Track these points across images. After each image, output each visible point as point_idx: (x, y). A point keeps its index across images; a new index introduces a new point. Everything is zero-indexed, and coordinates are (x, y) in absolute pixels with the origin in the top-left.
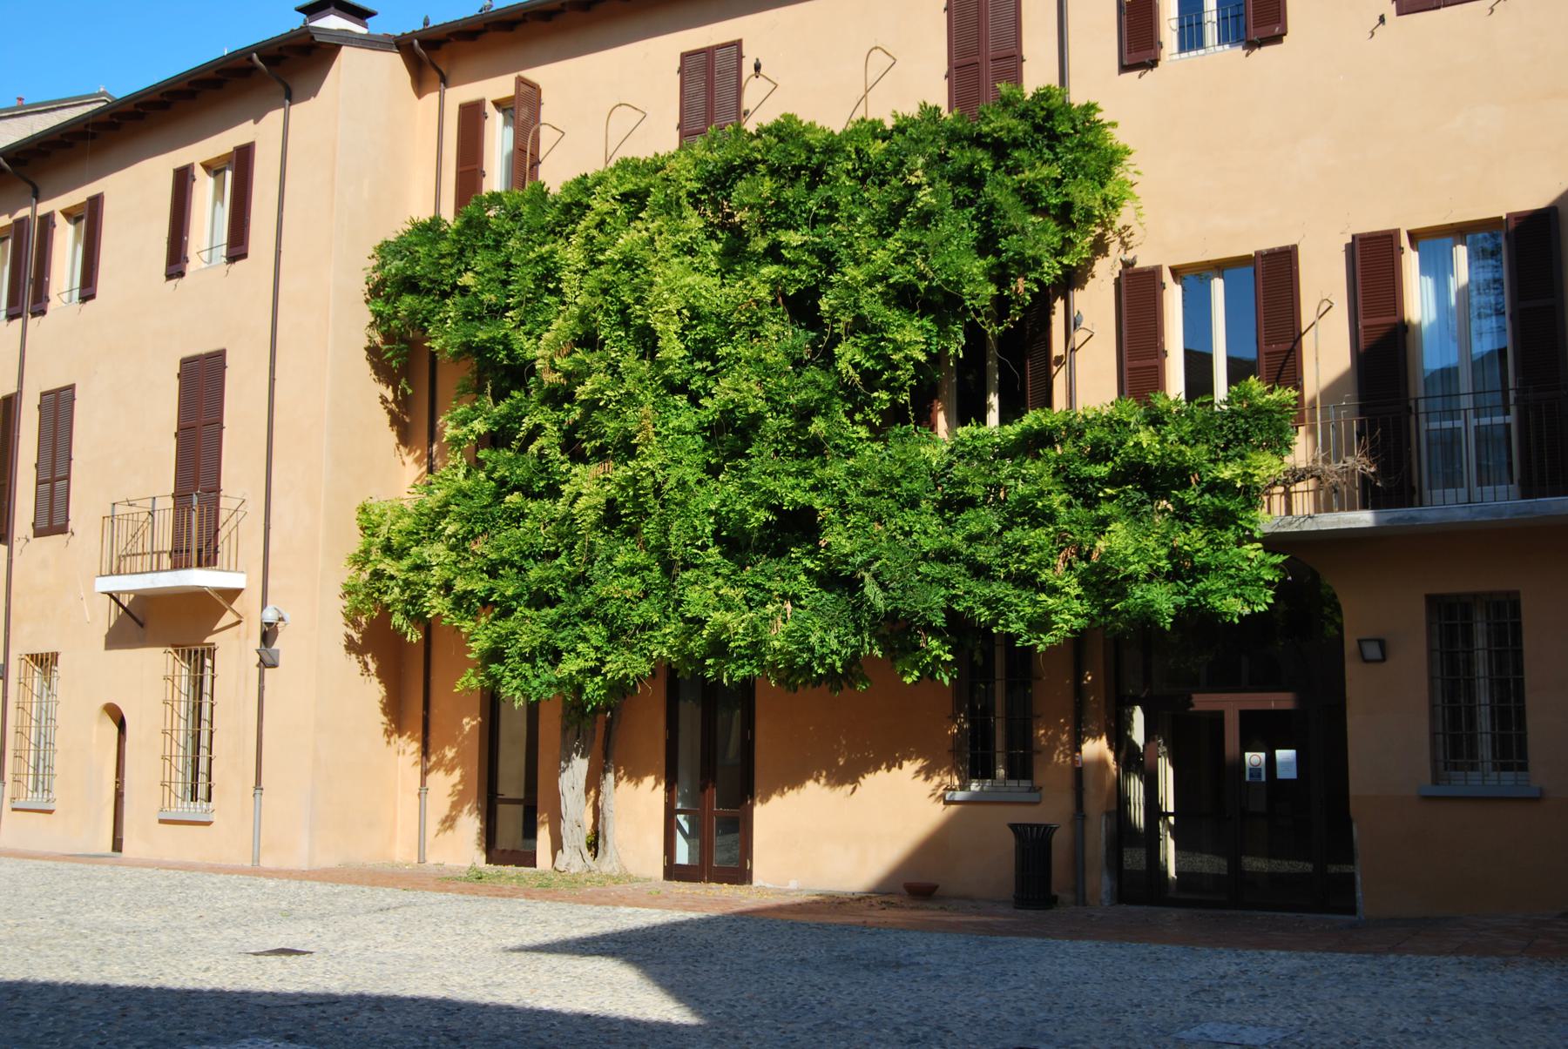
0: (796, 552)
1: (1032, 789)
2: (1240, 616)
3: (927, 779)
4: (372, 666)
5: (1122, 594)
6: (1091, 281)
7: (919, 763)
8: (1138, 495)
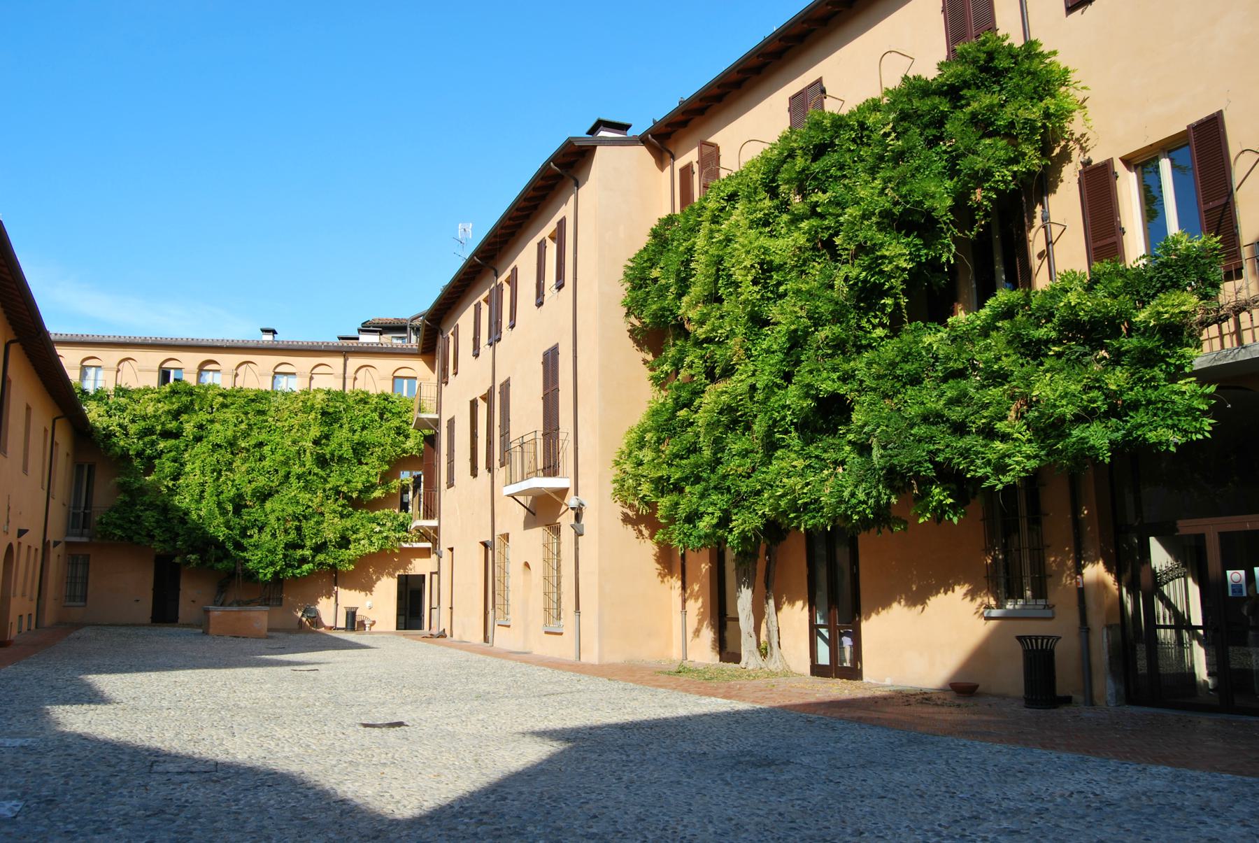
0: (842, 429)
1: (1046, 607)
2: (1176, 444)
3: (972, 600)
4: (646, 533)
5: (1064, 436)
6: (1061, 185)
7: (966, 588)
8: (1081, 349)
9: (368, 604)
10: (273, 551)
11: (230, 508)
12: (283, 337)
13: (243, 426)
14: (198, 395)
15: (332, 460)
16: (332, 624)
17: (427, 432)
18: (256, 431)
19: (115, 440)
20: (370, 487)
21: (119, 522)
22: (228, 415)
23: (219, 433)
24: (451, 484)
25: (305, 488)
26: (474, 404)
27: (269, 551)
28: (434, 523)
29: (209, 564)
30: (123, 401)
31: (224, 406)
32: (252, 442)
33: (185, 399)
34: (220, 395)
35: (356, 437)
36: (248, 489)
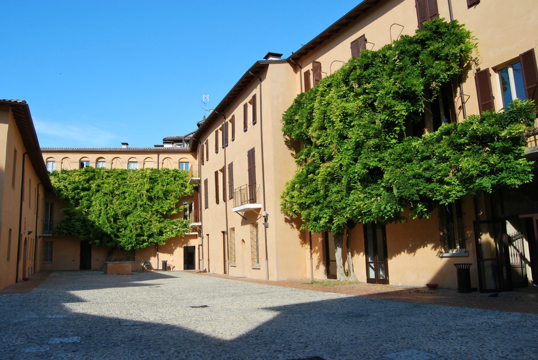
0: (379, 181)
1: (466, 252)
3: (435, 250)
6: (468, 79)
7: (432, 245)
8: (478, 147)
9: (171, 259)
10: (131, 238)
11: (112, 220)
12: (132, 146)
13: (116, 185)
14: (97, 172)
15: (155, 198)
16: (156, 268)
17: (194, 185)
18: (122, 187)
19: (62, 192)
20: (172, 209)
21: (65, 227)
22: (110, 180)
23: (106, 188)
24: (207, 207)
25: (144, 210)
26: (216, 173)
27: (129, 238)
28: (200, 224)
29: (104, 244)
30: (65, 176)
31: (108, 176)
32: (121, 192)
33: (91, 174)
34: (106, 172)
35: (165, 188)
36: (119, 212)
